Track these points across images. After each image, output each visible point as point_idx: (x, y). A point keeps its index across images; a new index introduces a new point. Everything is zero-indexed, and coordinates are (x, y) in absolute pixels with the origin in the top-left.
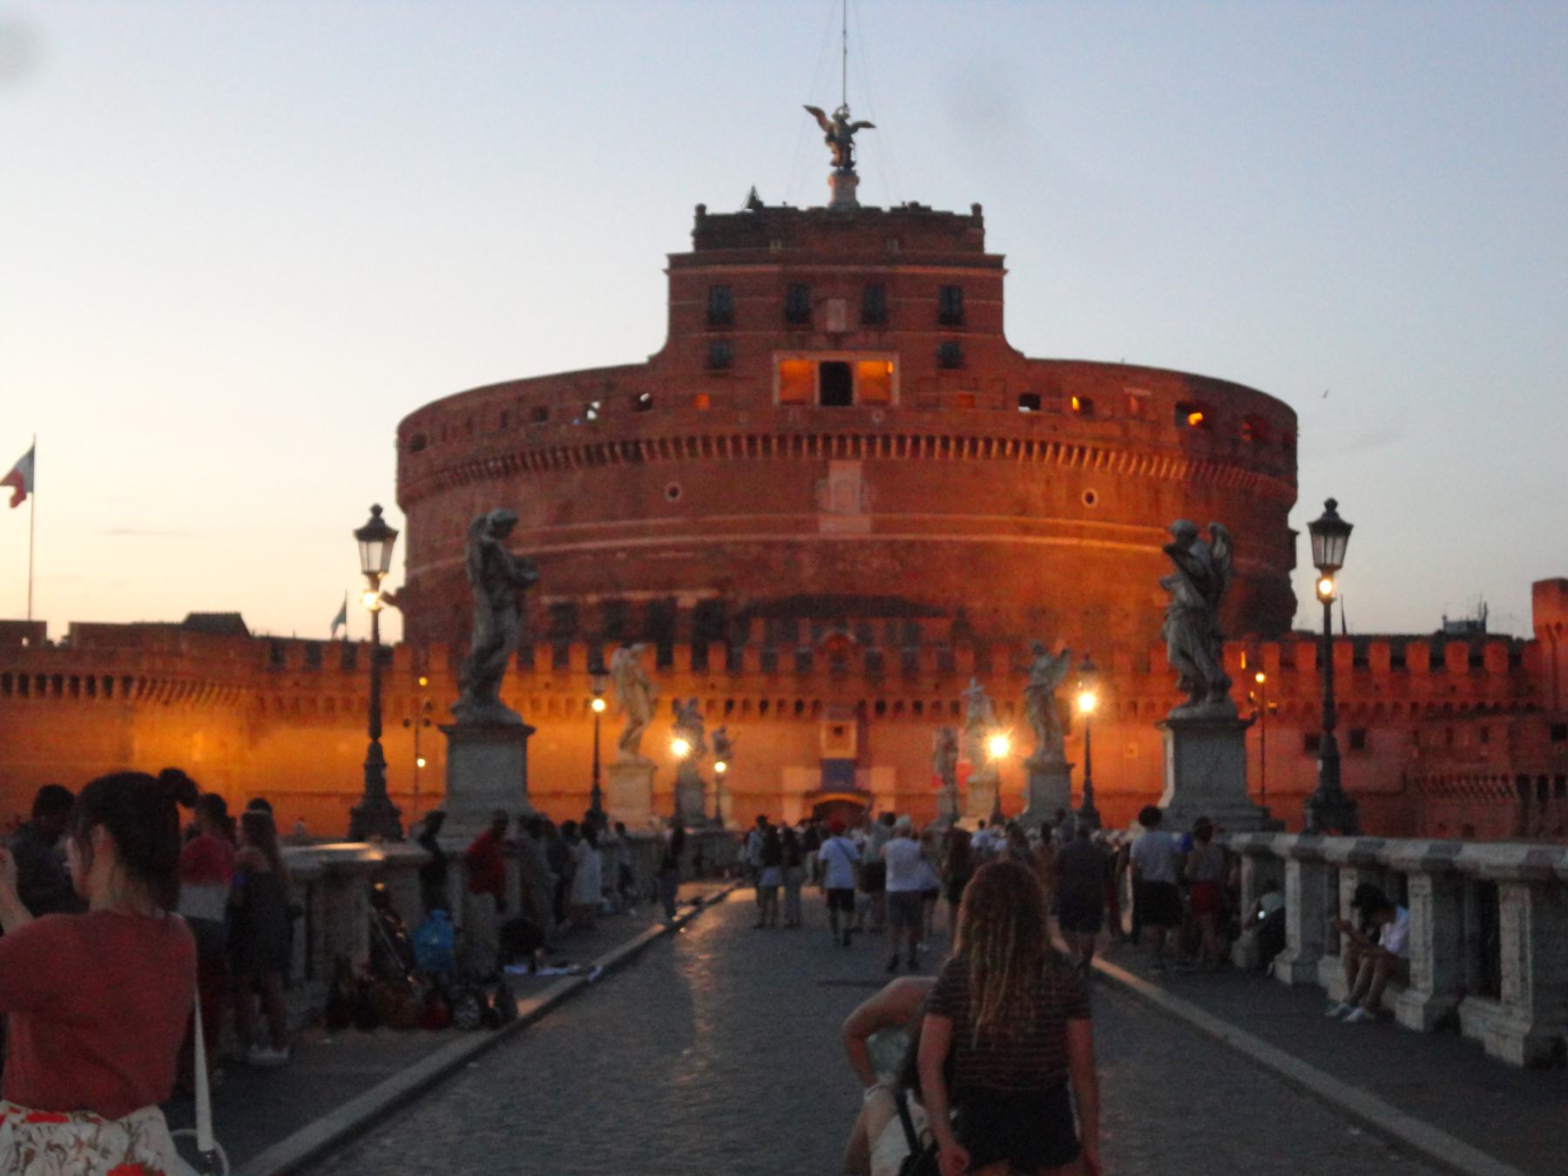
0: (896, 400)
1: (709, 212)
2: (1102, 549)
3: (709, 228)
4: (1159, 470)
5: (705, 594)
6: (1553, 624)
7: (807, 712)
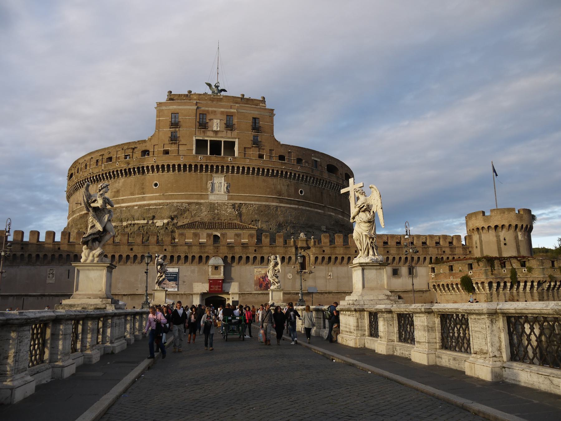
0: (236, 154)
1: (172, 93)
2: (306, 210)
3: (172, 97)
4: (322, 185)
5: (166, 221)
6: (480, 228)
7: (204, 260)
